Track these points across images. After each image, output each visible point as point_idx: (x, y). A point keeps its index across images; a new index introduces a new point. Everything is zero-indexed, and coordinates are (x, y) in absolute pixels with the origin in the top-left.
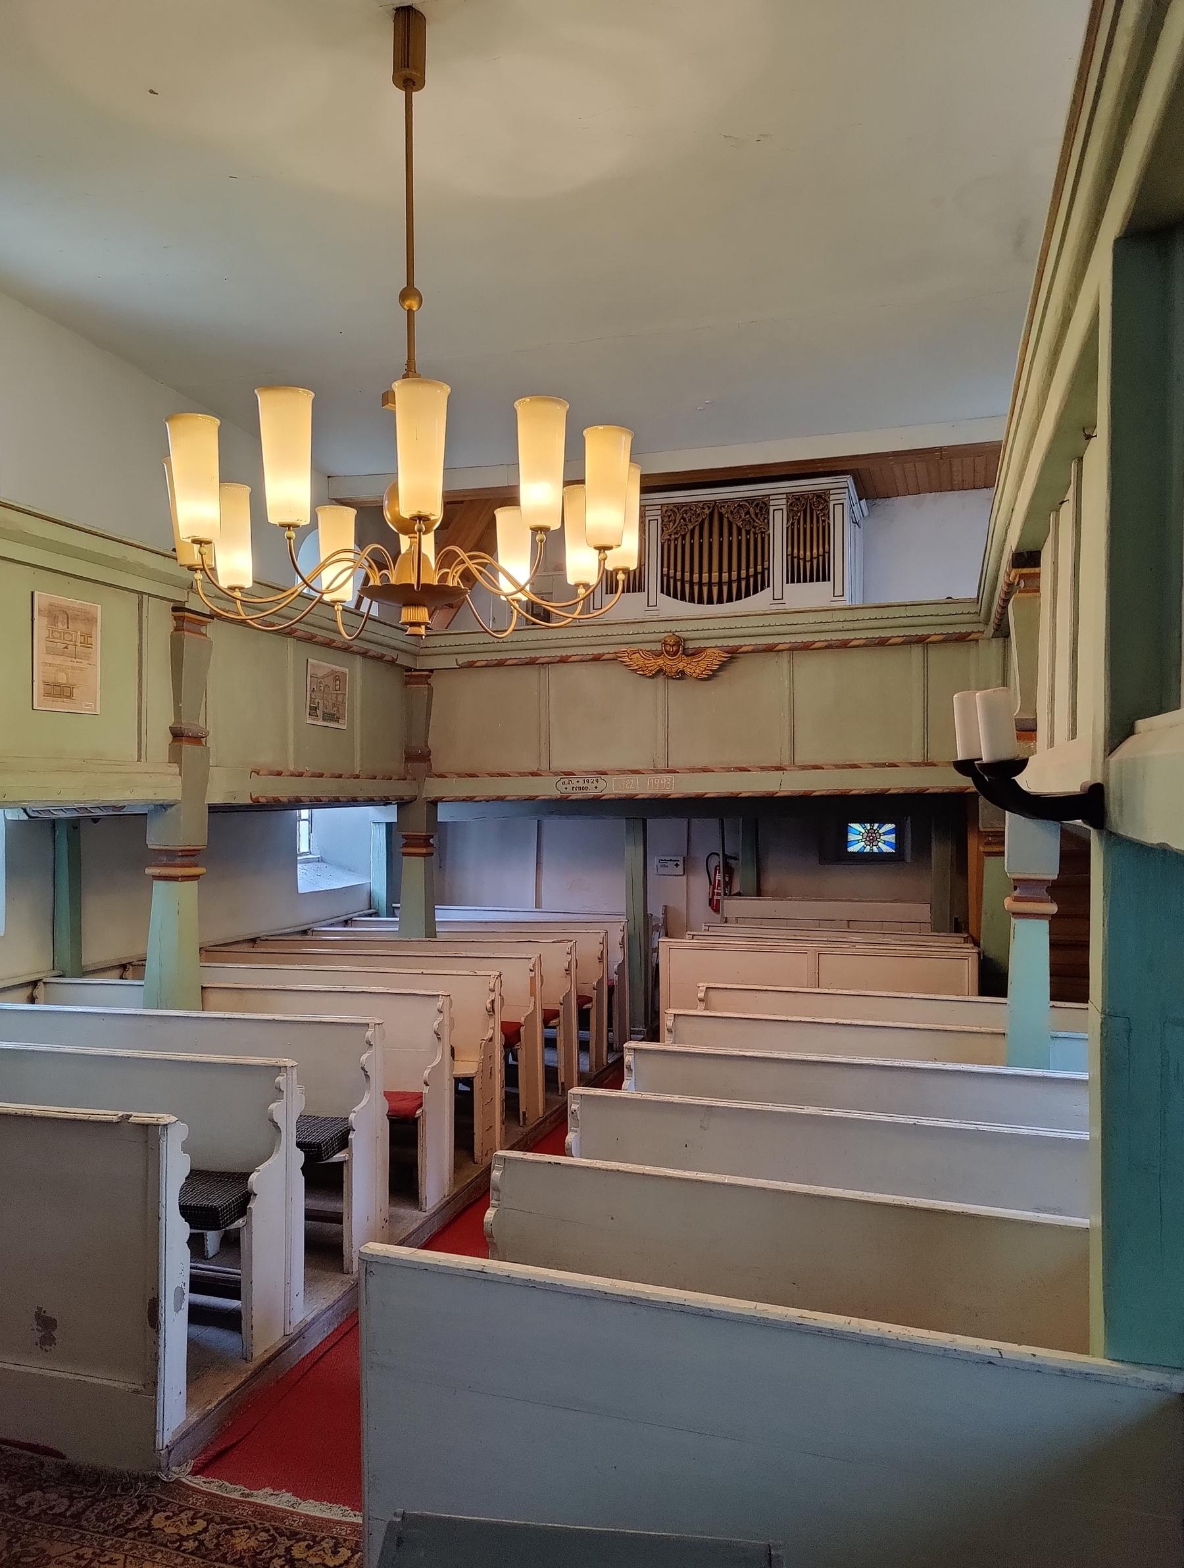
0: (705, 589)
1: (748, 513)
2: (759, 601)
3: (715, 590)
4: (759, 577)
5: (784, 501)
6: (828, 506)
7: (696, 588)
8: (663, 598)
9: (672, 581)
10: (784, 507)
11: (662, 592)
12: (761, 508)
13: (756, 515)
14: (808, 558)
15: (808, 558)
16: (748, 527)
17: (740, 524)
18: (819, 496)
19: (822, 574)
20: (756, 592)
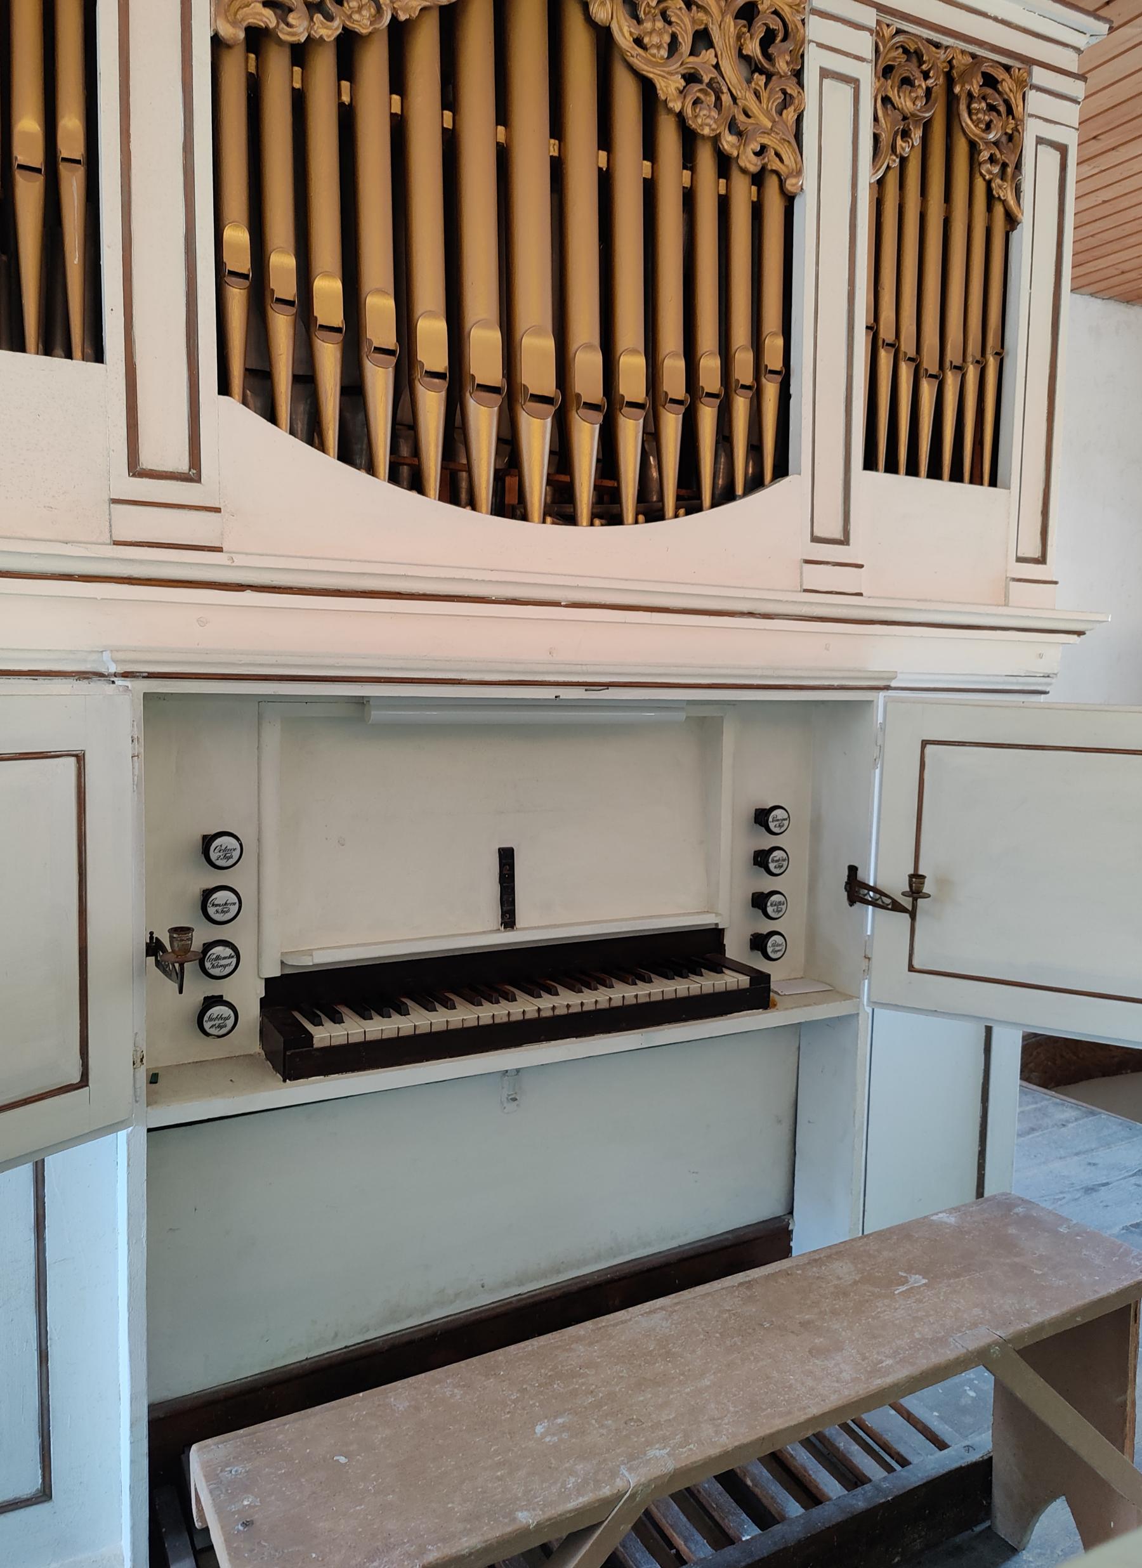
0: (483, 420)
1: (702, 38)
2: (744, 541)
3: (535, 435)
4: (741, 406)
5: (864, 44)
6: (1013, 138)
7: (431, 405)
8: (230, 420)
9: (282, 325)
10: (866, 74)
11: (224, 388)
12: (768, 40)
13: (752, 66)
14: (930, 362)
15: (930, 362)
16: (706, 122)
17: (669, 86)
18: (990, 81)
19: (966, 454)
20: (756, 483)
